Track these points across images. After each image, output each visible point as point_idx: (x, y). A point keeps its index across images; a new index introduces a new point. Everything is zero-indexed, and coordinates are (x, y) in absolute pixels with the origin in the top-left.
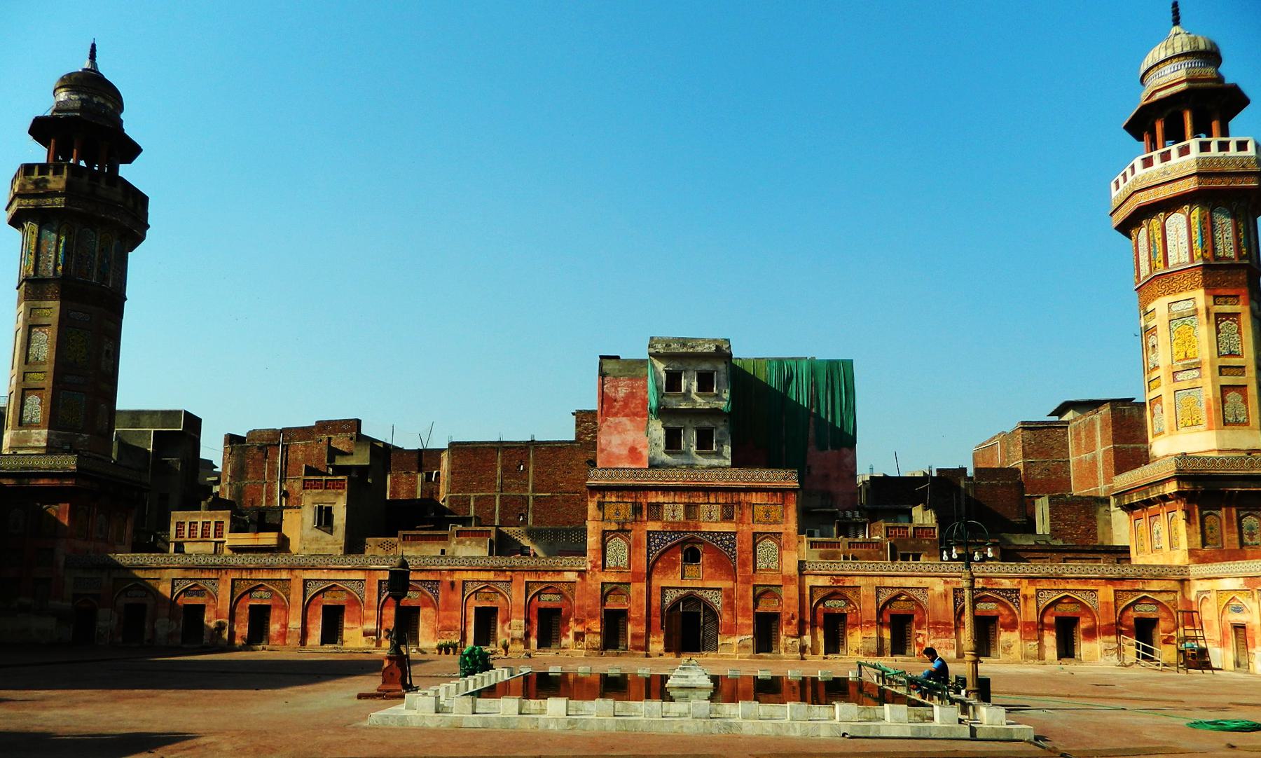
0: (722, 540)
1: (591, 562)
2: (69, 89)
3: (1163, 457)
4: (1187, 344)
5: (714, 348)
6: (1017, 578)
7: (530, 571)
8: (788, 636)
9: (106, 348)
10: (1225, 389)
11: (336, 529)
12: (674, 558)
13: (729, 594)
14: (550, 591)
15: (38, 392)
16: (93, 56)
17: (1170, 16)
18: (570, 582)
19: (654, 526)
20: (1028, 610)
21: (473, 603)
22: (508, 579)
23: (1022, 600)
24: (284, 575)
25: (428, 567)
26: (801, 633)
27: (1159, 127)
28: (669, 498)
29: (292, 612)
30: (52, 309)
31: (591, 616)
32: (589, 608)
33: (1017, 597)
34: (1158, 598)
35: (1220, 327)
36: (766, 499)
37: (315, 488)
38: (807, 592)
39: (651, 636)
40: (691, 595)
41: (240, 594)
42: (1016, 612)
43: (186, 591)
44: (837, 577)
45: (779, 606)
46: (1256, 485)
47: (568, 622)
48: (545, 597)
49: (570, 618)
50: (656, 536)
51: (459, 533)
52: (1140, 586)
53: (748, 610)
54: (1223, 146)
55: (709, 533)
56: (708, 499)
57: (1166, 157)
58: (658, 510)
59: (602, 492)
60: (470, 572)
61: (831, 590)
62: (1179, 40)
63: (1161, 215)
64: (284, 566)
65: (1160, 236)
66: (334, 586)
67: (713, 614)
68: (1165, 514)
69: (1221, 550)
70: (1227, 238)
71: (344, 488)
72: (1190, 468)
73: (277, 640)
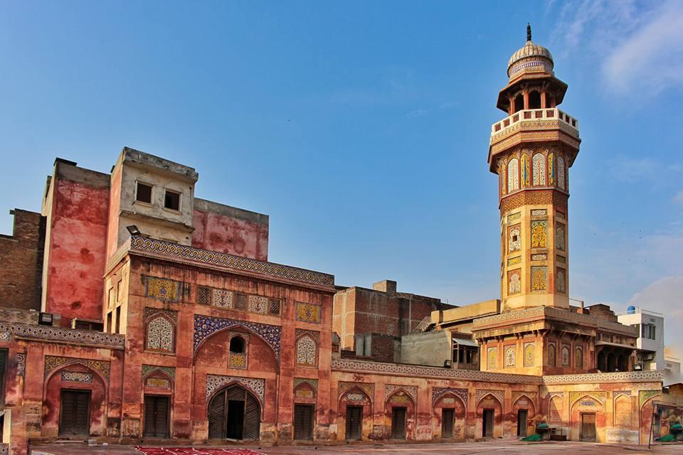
0: (267, 332)
1: (131, 341)
13: (271, 386)
14: (78, 369)
18: (102, 361)
19: (202, 310)
31: (131, 401)
36: (308, 299)
44: (359, 375)
45: (314, 397)
47: (99, 407)
48: (73, 376)
49: (102, 402)
50: (204, 321)
61: (353, 386)
67: (256, 404)
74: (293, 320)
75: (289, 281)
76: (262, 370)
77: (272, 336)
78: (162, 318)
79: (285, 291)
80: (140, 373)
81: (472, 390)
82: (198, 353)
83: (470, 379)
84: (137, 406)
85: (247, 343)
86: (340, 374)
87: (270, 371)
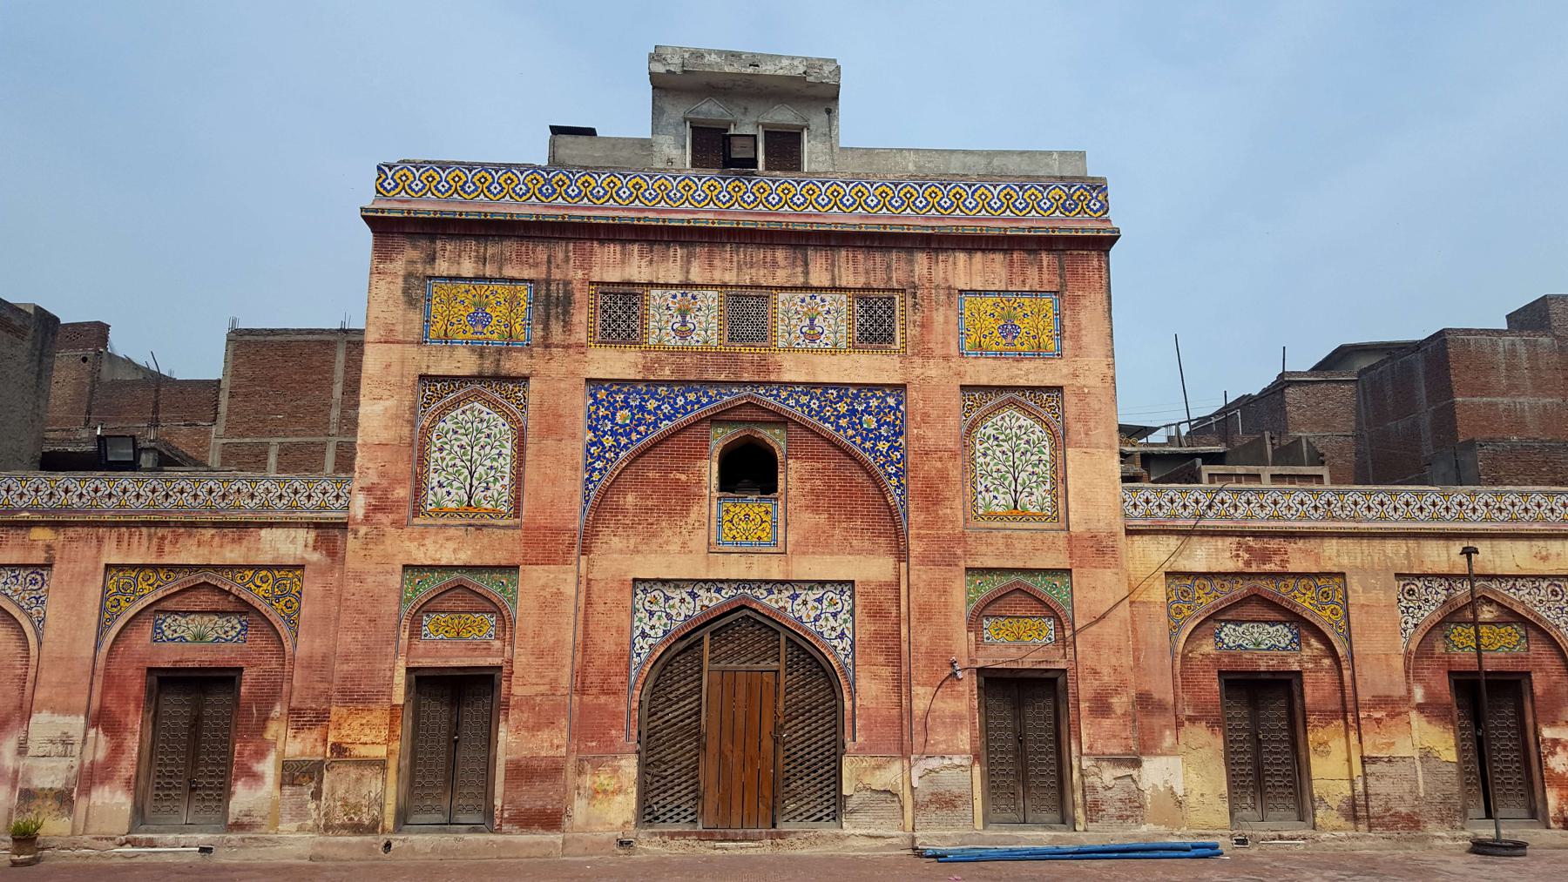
0: (853, 412)
1: (368, 490)
7: (128, 524)
8: (1099, 758)
12: (683, 477)
14: (205, 600)
18: (280, 567)
22: (38, 557)
28: (670, 267)
31: (358, 697)
40: (743, 607)
45: (1062, 642)
47: (264, 720)
48: (188, 627)
56: (806, 273)
59: (424, 243)
61: (1241, 589)
76: (842, 551)
77: (870, 422)
78: (477, 405)
79: (911, 262)
80: (394, 597)
82: (601, 508)
84: (379, 716)
85: (780, 456)
86: (1173, 542)
87: (871, 552)
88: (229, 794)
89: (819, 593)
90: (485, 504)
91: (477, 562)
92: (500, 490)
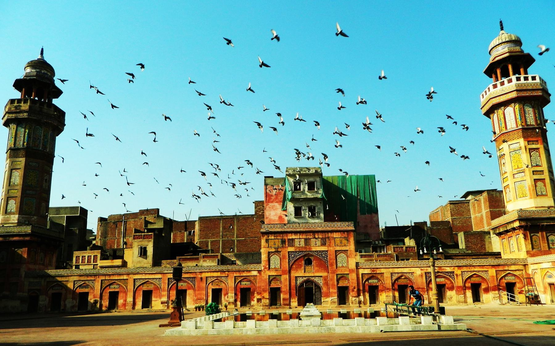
1: (264, 266)
2: (31, 67)
3: (512, 211)
4: (518, 162)
5: (314, 171)
6: (453, 266)
7: (236, 271)
8: (353, 297)
9: (45, 178)
10: (536, 181)
11: (149, 256)
12: (300, 263)
13: (325, 279)
14: (246, 280)
15: (14, 198)
16: (42, 53)
17: (499, 27)
19: (291, 249)
20: (458, 281)
21: (211, 287)
23: (455, 276)
24: (125, 277)
25: (191, 271)
26: (359, 295)
27: (498, 72)
28: (297, 236)
29: (129, 294)
30: (21, 161)
31: (264, 291)
32: (263, 287)
33: (453, 275)
34: (515, 273)
35: (531, 154)
36: (340, 235)
37: (139, 239)
38: (360, 276)
39: (292, 299)
40: (308, 280)
41: (105, 287)
42: (453, 282)
43: (80, 286)
45: (348, 283)
46: (553, 222)
47: (254, 294)
48: (243, 283)
50: (292, 253)
51: (204, 257)
52: (506, 268)
53: (334, 285)
54: (526, 79)
55: (316, 251)
57: (502, 84)
58: (292, 242)
59: (268, 235)
60: (209, 273)
61: (371, 275)
62: (504, 36)
63: (502, 108)
64: (125, 273)
65: (503, 117)
66: (148, 281)
67: (318, 288)
68: (515, 236)
69: (541, 251)
70: (531, 117)
71: (152, 238)
72: (524, 215)
73: (122, 307)
74: (333, 247)
75: (329, 229)
76: (321, 272)
81: (458, 272)
83: (455, 265)
86: (362, 270)
87: (325, 272)
88: (251, 302)
89: (318, 278)
90: (277, 268)
91: (277, 275)
92: (279, 266)
